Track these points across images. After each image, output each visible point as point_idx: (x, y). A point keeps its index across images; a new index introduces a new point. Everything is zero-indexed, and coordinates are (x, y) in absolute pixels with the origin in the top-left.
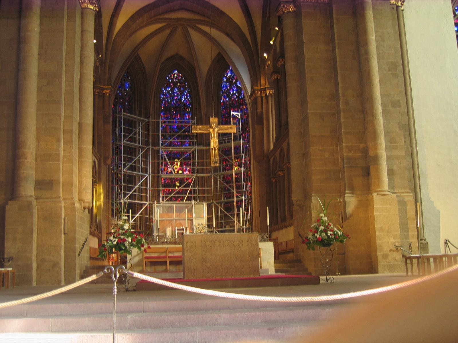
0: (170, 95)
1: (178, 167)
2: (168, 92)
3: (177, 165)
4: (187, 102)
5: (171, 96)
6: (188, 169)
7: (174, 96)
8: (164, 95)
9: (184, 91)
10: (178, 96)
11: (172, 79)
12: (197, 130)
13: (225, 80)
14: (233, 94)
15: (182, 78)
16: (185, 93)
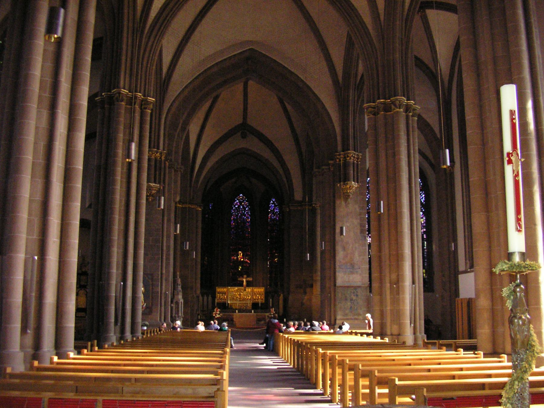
0: (237, 210)
1: (241, 256)
2: (236, 208)
3: (240, 255)
4: (248, 215)
5: (238, 211)
6: (247, 258)
7: (240, 211)
8: (234, 210)
9: (246, 208)
10: (242, 211)
11: (239, 200)
12: (239, 279)
13: (272, 202)
14: (277, 212)
15: (245, 199)
16: (247, 209)
